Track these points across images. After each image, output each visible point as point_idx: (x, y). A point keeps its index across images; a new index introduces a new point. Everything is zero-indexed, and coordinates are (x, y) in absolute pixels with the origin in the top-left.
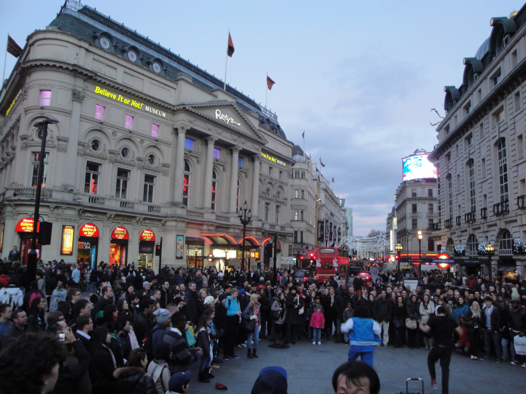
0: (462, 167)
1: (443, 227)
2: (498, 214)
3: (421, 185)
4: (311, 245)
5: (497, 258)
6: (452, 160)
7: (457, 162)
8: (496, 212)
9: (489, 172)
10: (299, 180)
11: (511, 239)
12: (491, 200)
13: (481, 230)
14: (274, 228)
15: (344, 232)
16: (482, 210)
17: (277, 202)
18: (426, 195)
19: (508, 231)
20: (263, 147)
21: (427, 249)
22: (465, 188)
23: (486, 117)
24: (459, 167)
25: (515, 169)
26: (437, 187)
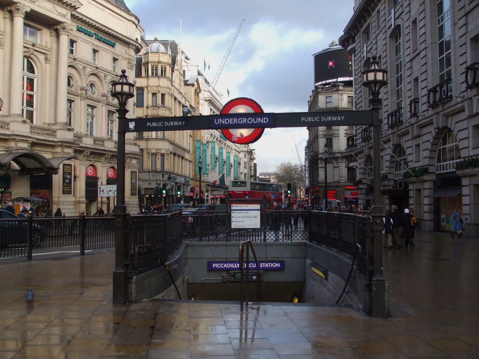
0: (384, 42)
1: (360, 141)
3: (338, 90)
4: (181, 176)
5: (433, 177)
6: (372, 36)
7: (379, 37)
8: (431, 103)
10: (157, 79)
14: (103, 145)
15: (245, 163)
16: (411, 102)
17: (108, 104)
20: (74, 13)
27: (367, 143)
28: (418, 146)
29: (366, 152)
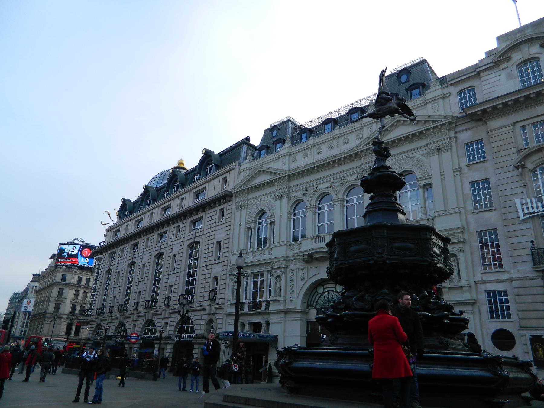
0: (124, 266)
2: (147, 308)
3: (73, 272)
6: (116, 258)
7: (120, 261)
9: (147, 275)
11: (154, 327)
12: (144, 296)
13: (131, 319)
18: (75, 281)
19: (153, 321)
21: (64, 333)
22: (123, 283)
23: (153, 234)
24: (121, 266)
25: (167, 277)
26: (95, 277)
27: (100, 317)
28: (135, 325)
29: (98, 321)
